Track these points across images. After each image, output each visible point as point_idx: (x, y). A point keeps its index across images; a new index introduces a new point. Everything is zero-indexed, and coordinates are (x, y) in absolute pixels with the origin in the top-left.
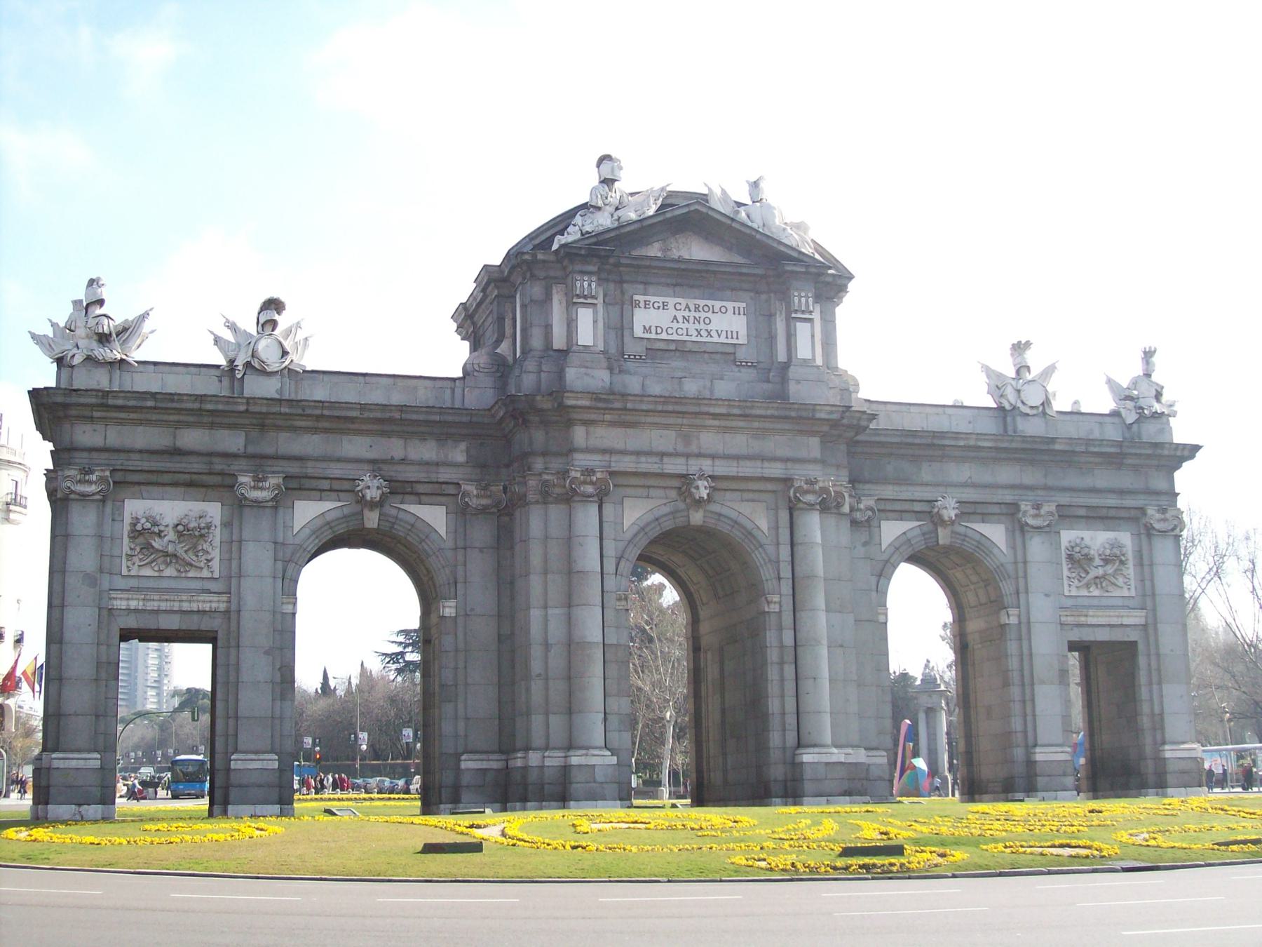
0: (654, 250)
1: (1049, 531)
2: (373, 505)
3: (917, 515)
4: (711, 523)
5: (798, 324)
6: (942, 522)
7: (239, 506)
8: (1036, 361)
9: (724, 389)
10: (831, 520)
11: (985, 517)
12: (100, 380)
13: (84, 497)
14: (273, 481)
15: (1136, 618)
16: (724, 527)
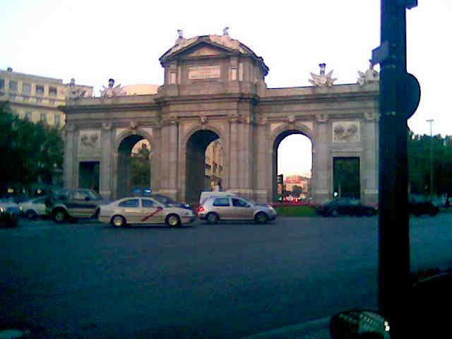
0: (195, 54)
1: (328, 123)
2: (132, 128)
3: (284, 121)
4: (209, 129)
5: (233, 70)
6: (291, 123)
7: (104, 131)
8: (327, 71)
9: (212, 92)
10: (241, 126)
11: (305, 120)
12: (73, 103)
13: (71, 132)
14: (110, 125)
15: (360, 149)
16: (212, 130)
